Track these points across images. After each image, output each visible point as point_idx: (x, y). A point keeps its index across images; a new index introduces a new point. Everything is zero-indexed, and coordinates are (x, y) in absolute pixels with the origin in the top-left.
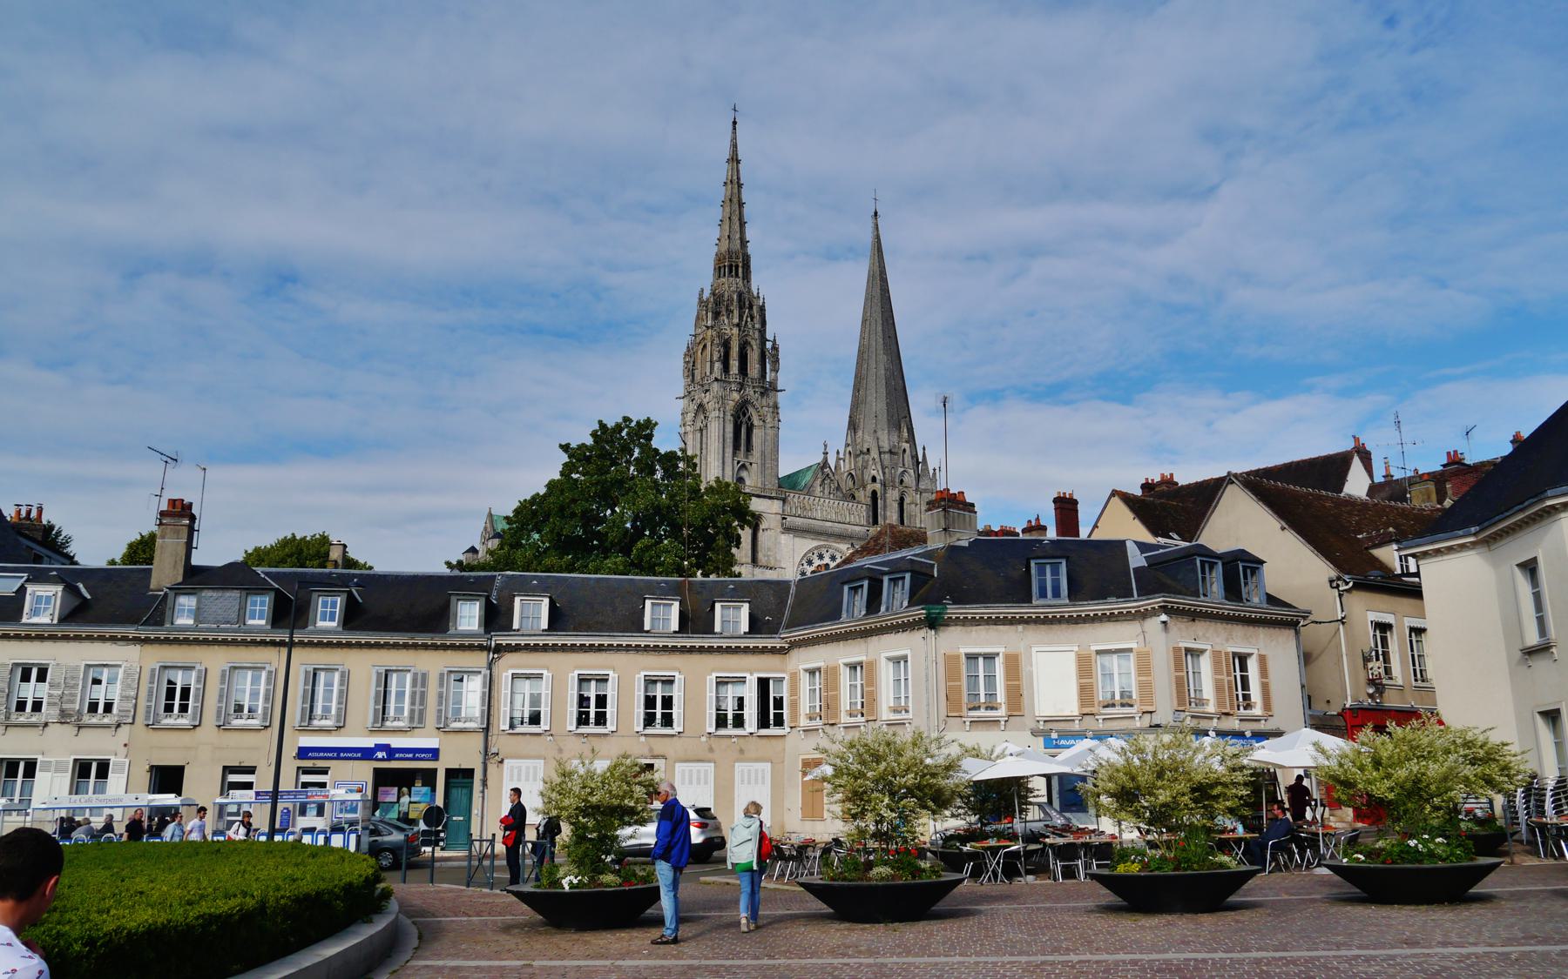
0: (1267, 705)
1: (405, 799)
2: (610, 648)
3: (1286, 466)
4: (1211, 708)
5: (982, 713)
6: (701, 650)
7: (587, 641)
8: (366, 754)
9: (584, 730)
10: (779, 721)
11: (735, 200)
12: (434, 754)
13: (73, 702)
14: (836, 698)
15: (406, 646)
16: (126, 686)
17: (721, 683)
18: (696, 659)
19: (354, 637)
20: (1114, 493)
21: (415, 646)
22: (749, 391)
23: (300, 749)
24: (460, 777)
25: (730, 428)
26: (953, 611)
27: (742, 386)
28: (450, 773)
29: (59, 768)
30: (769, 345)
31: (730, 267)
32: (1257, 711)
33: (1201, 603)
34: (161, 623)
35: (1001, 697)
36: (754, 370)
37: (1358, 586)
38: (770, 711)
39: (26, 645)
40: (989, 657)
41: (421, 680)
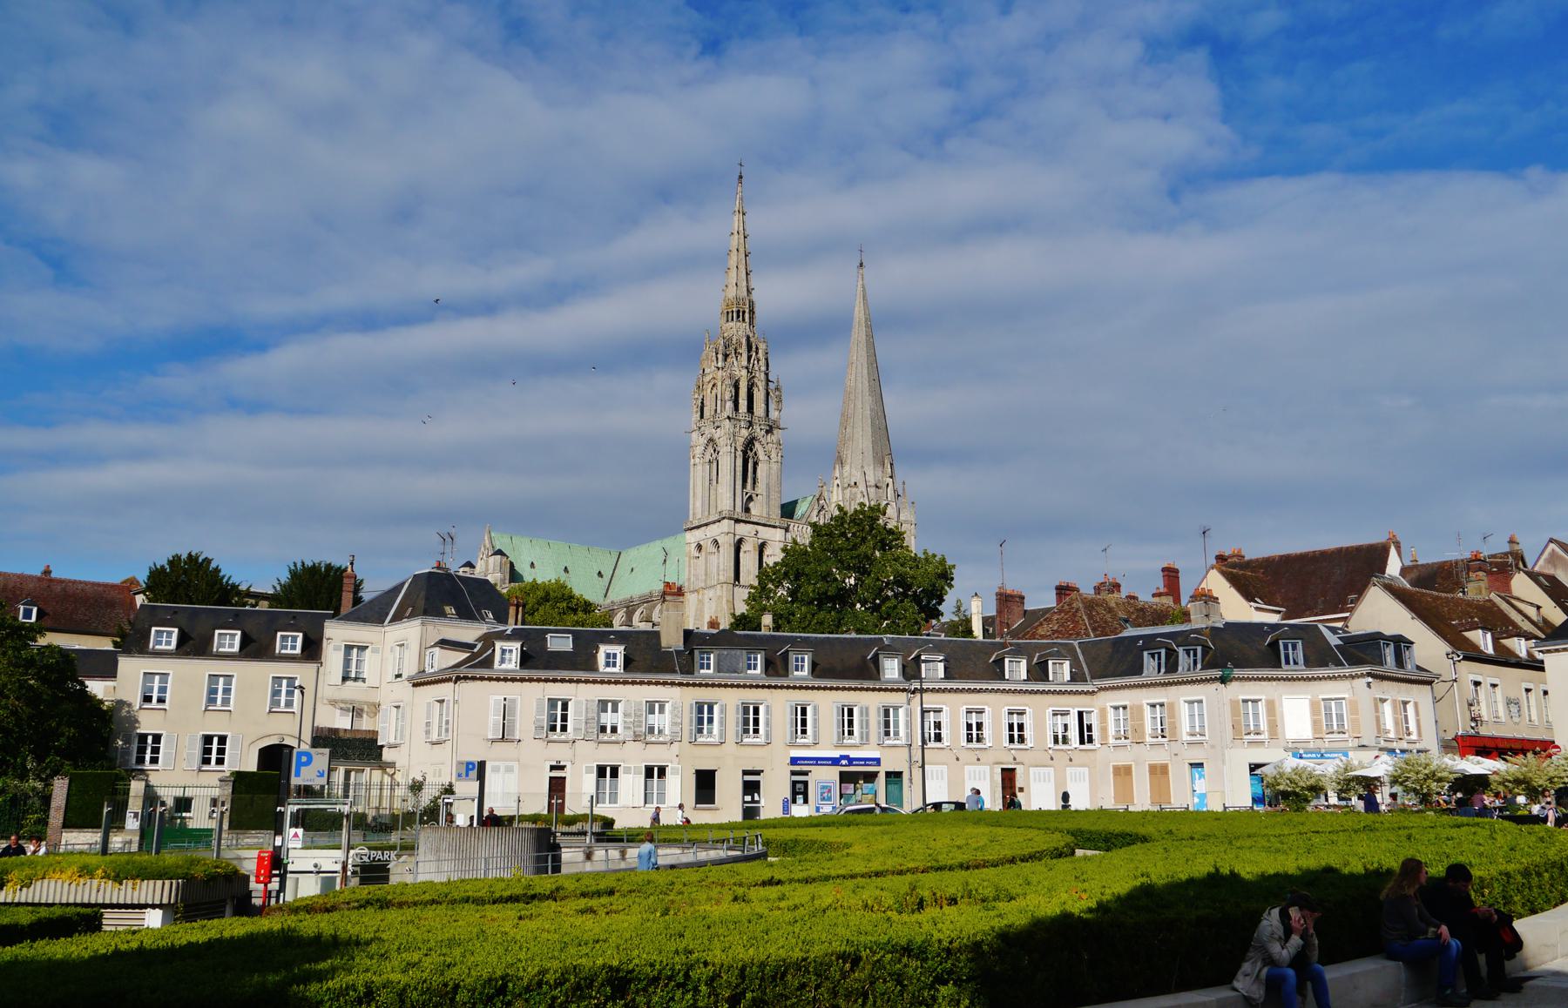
0: (1419, 734)
3: (1339, 551)
4: (1392, 735)
5: (1252, 736)
8: (835, 762)
9: (970, 745)
10: (1090, 740)
11: (742, 250)
12: (878, 761)
14: (1142, 726)
15: (856, 689)
16: (674, 715)
18: (1038, 697)
19: (817, 683)
21: (862, 689)
24: (894, 777)
25: (740, 462)
26: (1237, 672)
27: (751, 424)
28: (888, 774)
32: (1414, 737)
35: (1264, 726)
37: (1465, 658)
38: (1085, 736)
41: (865, 712)
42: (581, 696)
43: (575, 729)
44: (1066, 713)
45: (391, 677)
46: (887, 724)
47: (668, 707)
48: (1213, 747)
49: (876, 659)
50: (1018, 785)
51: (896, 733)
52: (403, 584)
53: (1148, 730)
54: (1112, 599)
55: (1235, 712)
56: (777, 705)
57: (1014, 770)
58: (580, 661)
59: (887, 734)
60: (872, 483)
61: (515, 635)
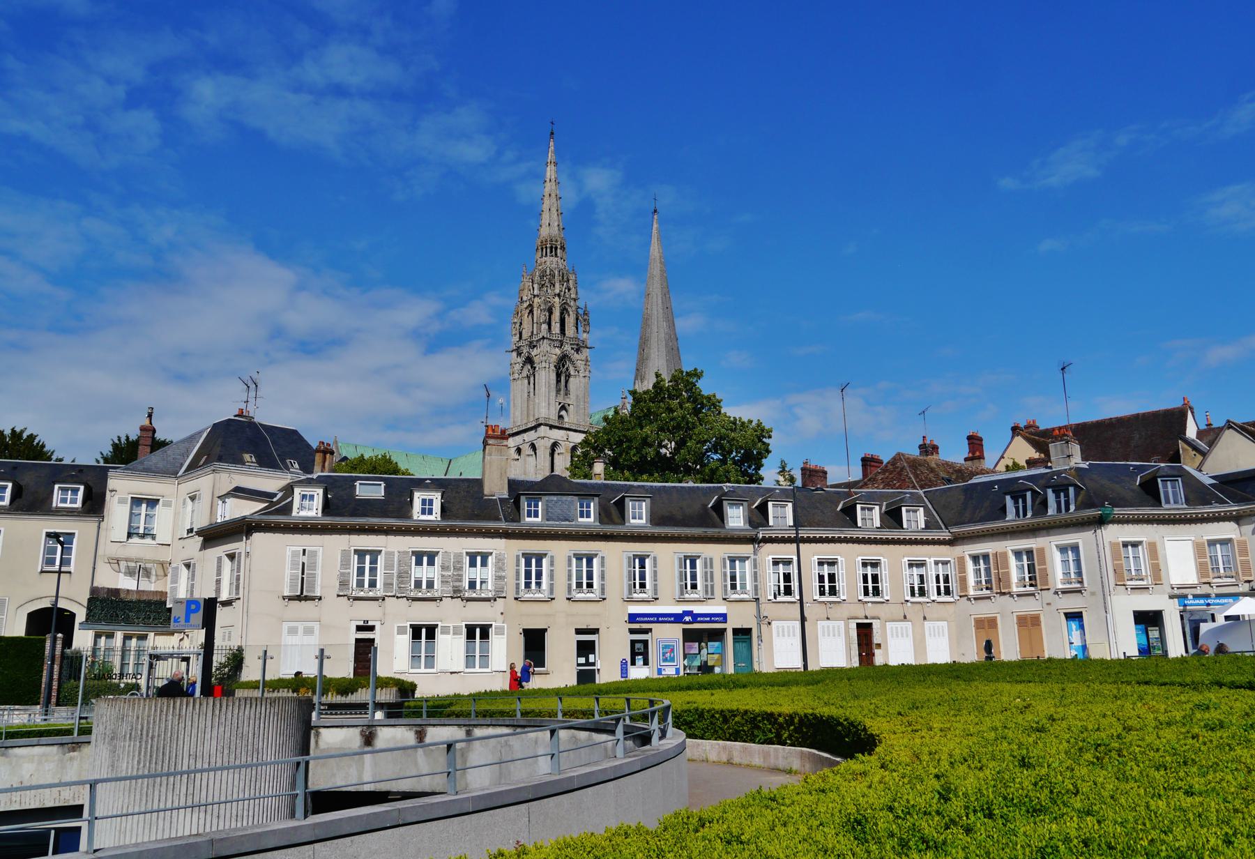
1: (704, 651)
8: (678, 618)
9: (823, 599)
12: (724, 617)
14: (1008, 574)
16: (500, 566)
17: (821, 563)
20: (1015, 430)
22: (567, 348)
24: (743, 634)
29: (456, 632)
33: (1167, 509)
35: (1145, 570)
36: (570, 331)
40: (1135, 545)
41: (709, 563)
44: (921, 564)
46: (733, 578)
47: (490, 560)
48: (1093, 594)
49: (719, 508)
50: (876, 639)
51: (743, 586)
52: (200, 433)
54: (932, 459)
55: (1116, 556)
56: (614, 558)
59: (734, 587)
61: (319, 481)
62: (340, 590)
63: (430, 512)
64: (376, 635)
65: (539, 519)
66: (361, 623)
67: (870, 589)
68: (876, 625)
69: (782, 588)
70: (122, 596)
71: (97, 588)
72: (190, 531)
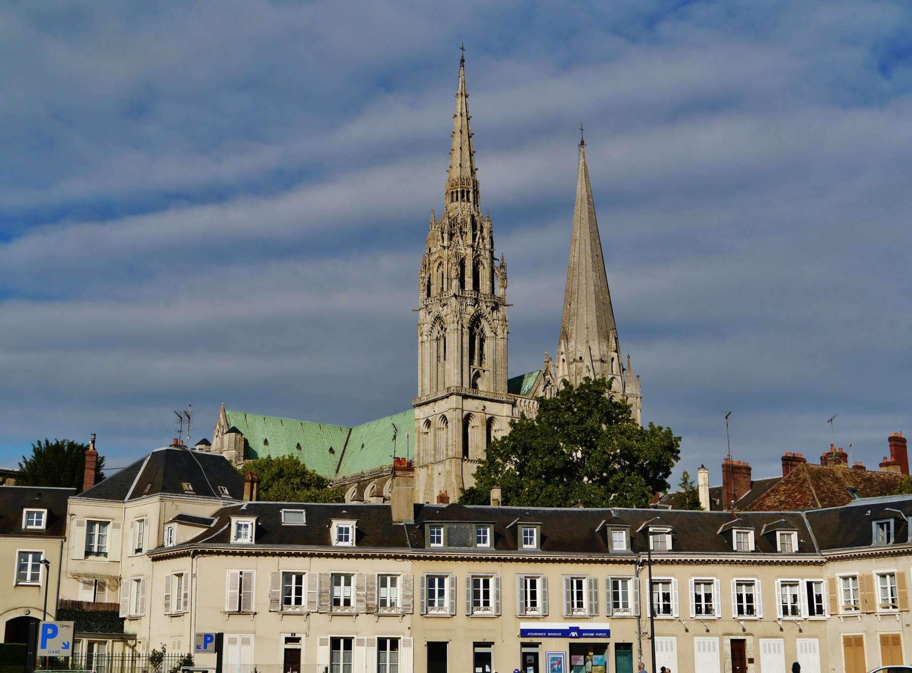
1: (589, 664)
2: (715, 562)
6: (771, 563)
7: (700, 558)
8: (565, 633)
9: (699, 617)
10: (820, 611)
11: (465, 131)
12: (607, 633)
13: (373, 599)
14: (873, 596)
15: (584, 562)
18: (766, 568)
19: (545, 556)
21: (590, 562)
23: (522, 630)
24: (624, 649)
27: (476, 301)
28: (618, 646)
29: (370, 645)
30: (497, 263)
31: (463, 192)
34: (423, 547)
36: (485, 286)
39: (338, 561)
41: (594, 584)
42: (315, 570)
43: (309, 602)
44: (794, 584)
45: (131, 552)
46: (616, 596)
47: (399, 580)
50: (749, 655)
51: (625, 605)
52: (143, 461)
53: (879, 600)
54: (839, 469)
56: (507, 577)
57: (744, 640)
58: (313, 537)
59: (616, 605)
60: (597, 356)
61: (249, 511)
62: (271, 606)
63: (347, 539)
64: (302, 646)
65: (441, 545)
66: (289, 636)
67: (745, 608)
68: (749, 641)
69: (661, 607)
70: (85, 607)
71: (62, 600)
72: (139, 550)
